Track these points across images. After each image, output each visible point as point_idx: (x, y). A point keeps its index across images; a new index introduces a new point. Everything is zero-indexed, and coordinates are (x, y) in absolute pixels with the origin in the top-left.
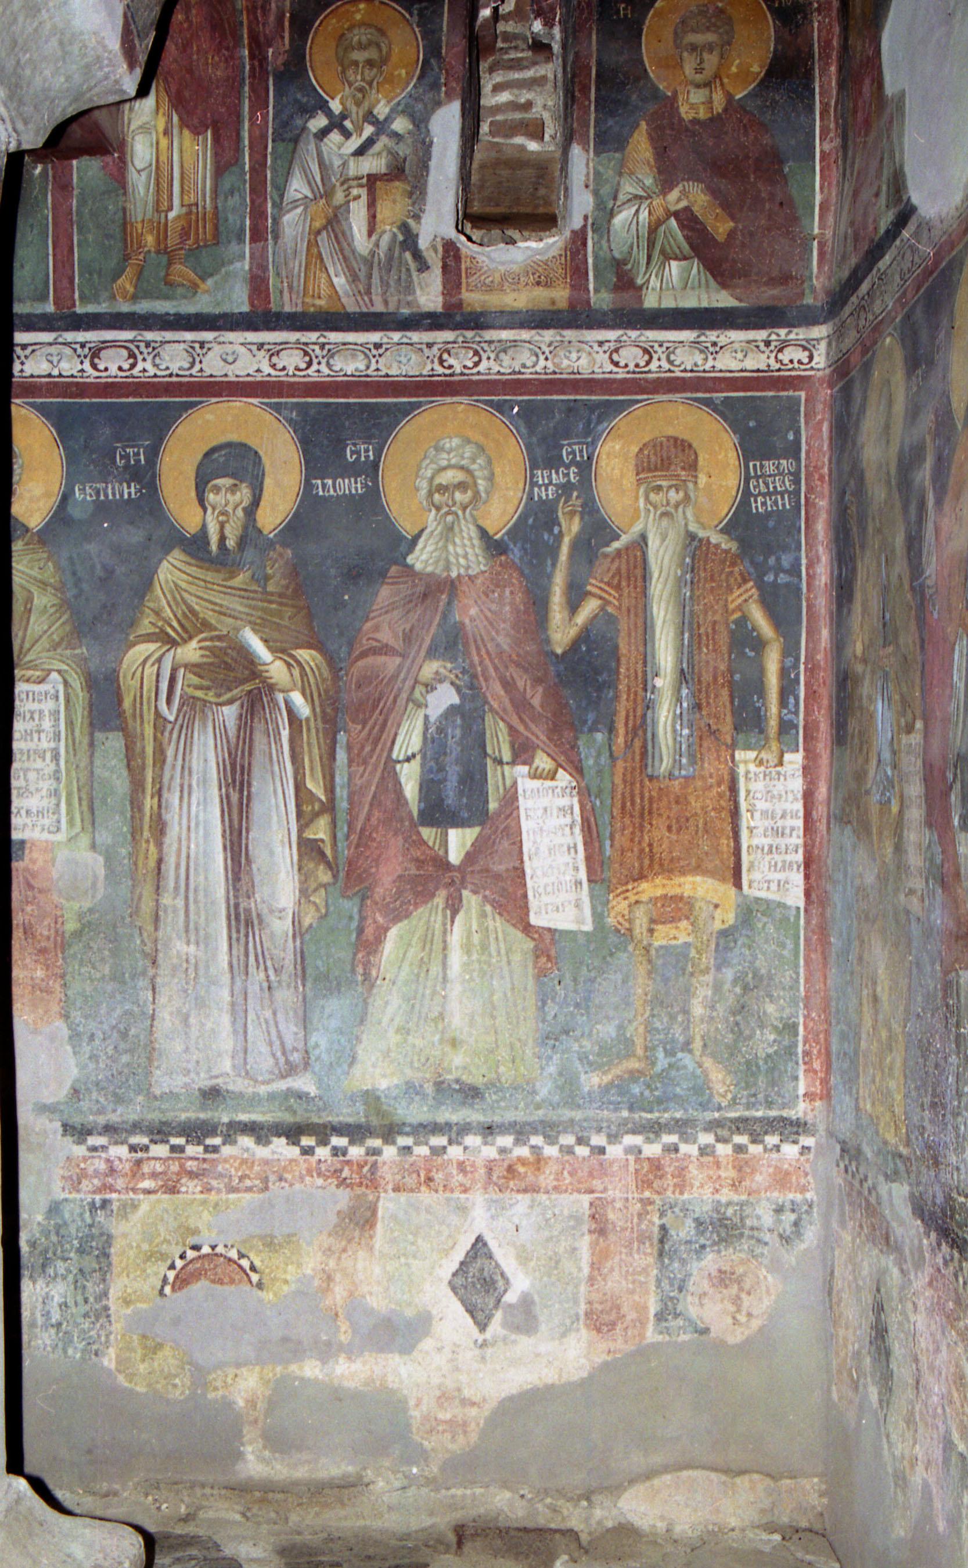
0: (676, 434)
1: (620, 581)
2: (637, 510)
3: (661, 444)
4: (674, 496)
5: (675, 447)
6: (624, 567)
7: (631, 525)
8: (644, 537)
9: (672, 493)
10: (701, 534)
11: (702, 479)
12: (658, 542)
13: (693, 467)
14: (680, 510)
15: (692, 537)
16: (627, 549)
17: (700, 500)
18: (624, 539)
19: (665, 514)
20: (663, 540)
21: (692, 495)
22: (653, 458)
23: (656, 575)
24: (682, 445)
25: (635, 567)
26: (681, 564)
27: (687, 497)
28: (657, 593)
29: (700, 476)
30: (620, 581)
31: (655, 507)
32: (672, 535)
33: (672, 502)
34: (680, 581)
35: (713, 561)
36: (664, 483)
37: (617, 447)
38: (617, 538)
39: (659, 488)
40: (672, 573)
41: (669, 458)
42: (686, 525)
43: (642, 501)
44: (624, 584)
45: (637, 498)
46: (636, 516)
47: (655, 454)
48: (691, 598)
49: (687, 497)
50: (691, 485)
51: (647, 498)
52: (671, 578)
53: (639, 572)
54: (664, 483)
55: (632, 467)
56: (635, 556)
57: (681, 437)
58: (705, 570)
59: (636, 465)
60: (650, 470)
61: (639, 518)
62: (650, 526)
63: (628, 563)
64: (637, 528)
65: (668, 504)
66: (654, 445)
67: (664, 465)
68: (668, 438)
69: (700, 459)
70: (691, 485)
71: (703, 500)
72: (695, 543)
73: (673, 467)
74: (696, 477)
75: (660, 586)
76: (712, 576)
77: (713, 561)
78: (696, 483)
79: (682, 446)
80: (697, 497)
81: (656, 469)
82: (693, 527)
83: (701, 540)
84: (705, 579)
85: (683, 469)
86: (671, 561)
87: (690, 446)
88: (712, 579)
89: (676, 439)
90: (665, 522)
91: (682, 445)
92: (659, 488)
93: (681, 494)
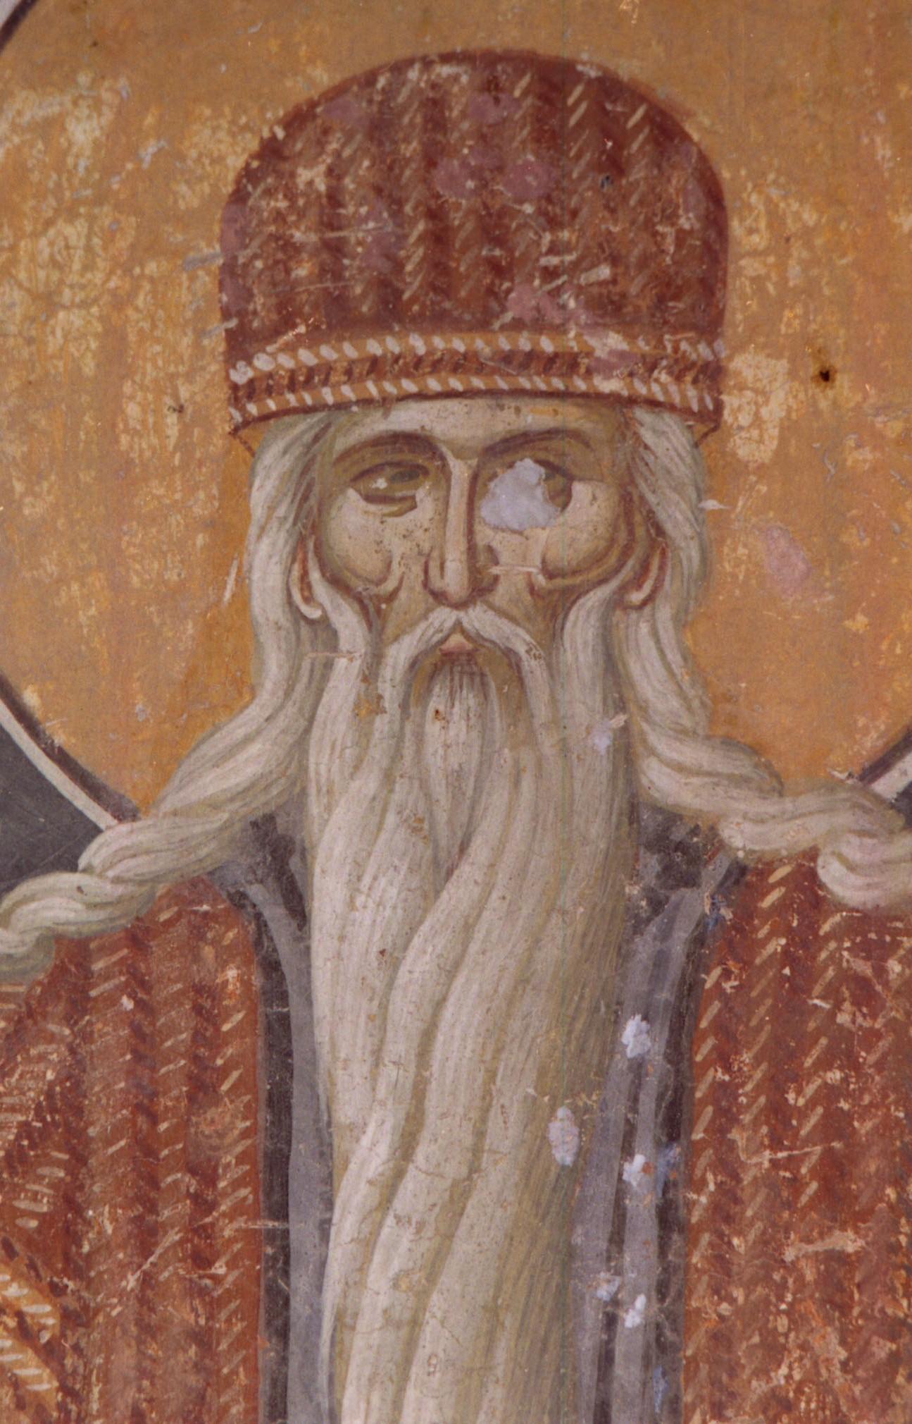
0: (546, 44)
1: (70, 1200)
2: (228, 635)
3: (435, 107)
4: (533, 524)
5: (549, 136)
6: (108, 1088)
7: (170, 756)
8: (276, 848)
9: (517, 496)
10: (751, 828)
11: (763, 397)
12: (389, 889)
13: (686, 293)
14: (581, 626)
15: (675, 848)
16: (138, 937)
17: (736, 556)
18: (121, 860)
19: (448, 664)
20: (440, 869)
21: (676, 516)
22: (365, 228)
23: (367, 1155)
24: (605, 124)
25: (202, 1088)
26: (581, 1069)
27: (637, 542)
28: (378, 1295)
29: (745, 365)
30: (70, 1200)
31: (374, 610)
32: (506, 825)
33: (517, 569)
34: (562, 1204)
35: (843, 1051)
36: (455, 423)
37: (84, 132)
38: (63, 845)
39: (411, 458)
40: (505, 1134)
41: (494, 226)
42: (626, 752)
43: (267, 562)
44: (105, 1221)
45: (228, 536)
46: (215, 679)
47: (387, 193)
48: (661, 1346)
49: (637, 542)
50: (666, 439)
51: (310, 538)
52: (498, 1176)
53: (229, 1125)
54: (455, 423)
55: (199, 288)
56: (205, 1002)
57: (589, 63)
58: (779, 1118)
59: (231, 272)
60: (339, 317)
61: (242, 688)
62: (322, 763)
63: (143, 1044)
64: (230, 769)
65: (480, 587)
66: (383, 116)
67: (451, 277)
68: (491, 68)
69: (748, 234)
70: (666, 439)
71: (761, 551)
72: (698, 902)
73: (523, 297)
74: (712, 374)
75: (398, 1249)
76: (835, 1172)
77: (843, 1051)
78: (709, 421)
79: (604, 126)
80: (714, 535)
81: (391, 311)
82: (678, 776)
83: (744, 878)
84: (782, 1189)
85: (608, 308)
86: (496, 1038)
87: (666, 130)
88: (837, 1201)
89: (553, 78)
90: (451, 731)
91: (605, 124)
92: (411, 458)
93: (590, 505)
